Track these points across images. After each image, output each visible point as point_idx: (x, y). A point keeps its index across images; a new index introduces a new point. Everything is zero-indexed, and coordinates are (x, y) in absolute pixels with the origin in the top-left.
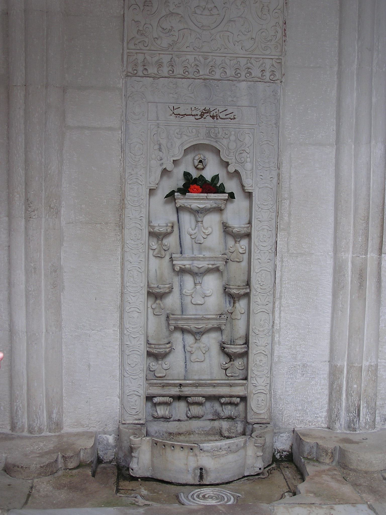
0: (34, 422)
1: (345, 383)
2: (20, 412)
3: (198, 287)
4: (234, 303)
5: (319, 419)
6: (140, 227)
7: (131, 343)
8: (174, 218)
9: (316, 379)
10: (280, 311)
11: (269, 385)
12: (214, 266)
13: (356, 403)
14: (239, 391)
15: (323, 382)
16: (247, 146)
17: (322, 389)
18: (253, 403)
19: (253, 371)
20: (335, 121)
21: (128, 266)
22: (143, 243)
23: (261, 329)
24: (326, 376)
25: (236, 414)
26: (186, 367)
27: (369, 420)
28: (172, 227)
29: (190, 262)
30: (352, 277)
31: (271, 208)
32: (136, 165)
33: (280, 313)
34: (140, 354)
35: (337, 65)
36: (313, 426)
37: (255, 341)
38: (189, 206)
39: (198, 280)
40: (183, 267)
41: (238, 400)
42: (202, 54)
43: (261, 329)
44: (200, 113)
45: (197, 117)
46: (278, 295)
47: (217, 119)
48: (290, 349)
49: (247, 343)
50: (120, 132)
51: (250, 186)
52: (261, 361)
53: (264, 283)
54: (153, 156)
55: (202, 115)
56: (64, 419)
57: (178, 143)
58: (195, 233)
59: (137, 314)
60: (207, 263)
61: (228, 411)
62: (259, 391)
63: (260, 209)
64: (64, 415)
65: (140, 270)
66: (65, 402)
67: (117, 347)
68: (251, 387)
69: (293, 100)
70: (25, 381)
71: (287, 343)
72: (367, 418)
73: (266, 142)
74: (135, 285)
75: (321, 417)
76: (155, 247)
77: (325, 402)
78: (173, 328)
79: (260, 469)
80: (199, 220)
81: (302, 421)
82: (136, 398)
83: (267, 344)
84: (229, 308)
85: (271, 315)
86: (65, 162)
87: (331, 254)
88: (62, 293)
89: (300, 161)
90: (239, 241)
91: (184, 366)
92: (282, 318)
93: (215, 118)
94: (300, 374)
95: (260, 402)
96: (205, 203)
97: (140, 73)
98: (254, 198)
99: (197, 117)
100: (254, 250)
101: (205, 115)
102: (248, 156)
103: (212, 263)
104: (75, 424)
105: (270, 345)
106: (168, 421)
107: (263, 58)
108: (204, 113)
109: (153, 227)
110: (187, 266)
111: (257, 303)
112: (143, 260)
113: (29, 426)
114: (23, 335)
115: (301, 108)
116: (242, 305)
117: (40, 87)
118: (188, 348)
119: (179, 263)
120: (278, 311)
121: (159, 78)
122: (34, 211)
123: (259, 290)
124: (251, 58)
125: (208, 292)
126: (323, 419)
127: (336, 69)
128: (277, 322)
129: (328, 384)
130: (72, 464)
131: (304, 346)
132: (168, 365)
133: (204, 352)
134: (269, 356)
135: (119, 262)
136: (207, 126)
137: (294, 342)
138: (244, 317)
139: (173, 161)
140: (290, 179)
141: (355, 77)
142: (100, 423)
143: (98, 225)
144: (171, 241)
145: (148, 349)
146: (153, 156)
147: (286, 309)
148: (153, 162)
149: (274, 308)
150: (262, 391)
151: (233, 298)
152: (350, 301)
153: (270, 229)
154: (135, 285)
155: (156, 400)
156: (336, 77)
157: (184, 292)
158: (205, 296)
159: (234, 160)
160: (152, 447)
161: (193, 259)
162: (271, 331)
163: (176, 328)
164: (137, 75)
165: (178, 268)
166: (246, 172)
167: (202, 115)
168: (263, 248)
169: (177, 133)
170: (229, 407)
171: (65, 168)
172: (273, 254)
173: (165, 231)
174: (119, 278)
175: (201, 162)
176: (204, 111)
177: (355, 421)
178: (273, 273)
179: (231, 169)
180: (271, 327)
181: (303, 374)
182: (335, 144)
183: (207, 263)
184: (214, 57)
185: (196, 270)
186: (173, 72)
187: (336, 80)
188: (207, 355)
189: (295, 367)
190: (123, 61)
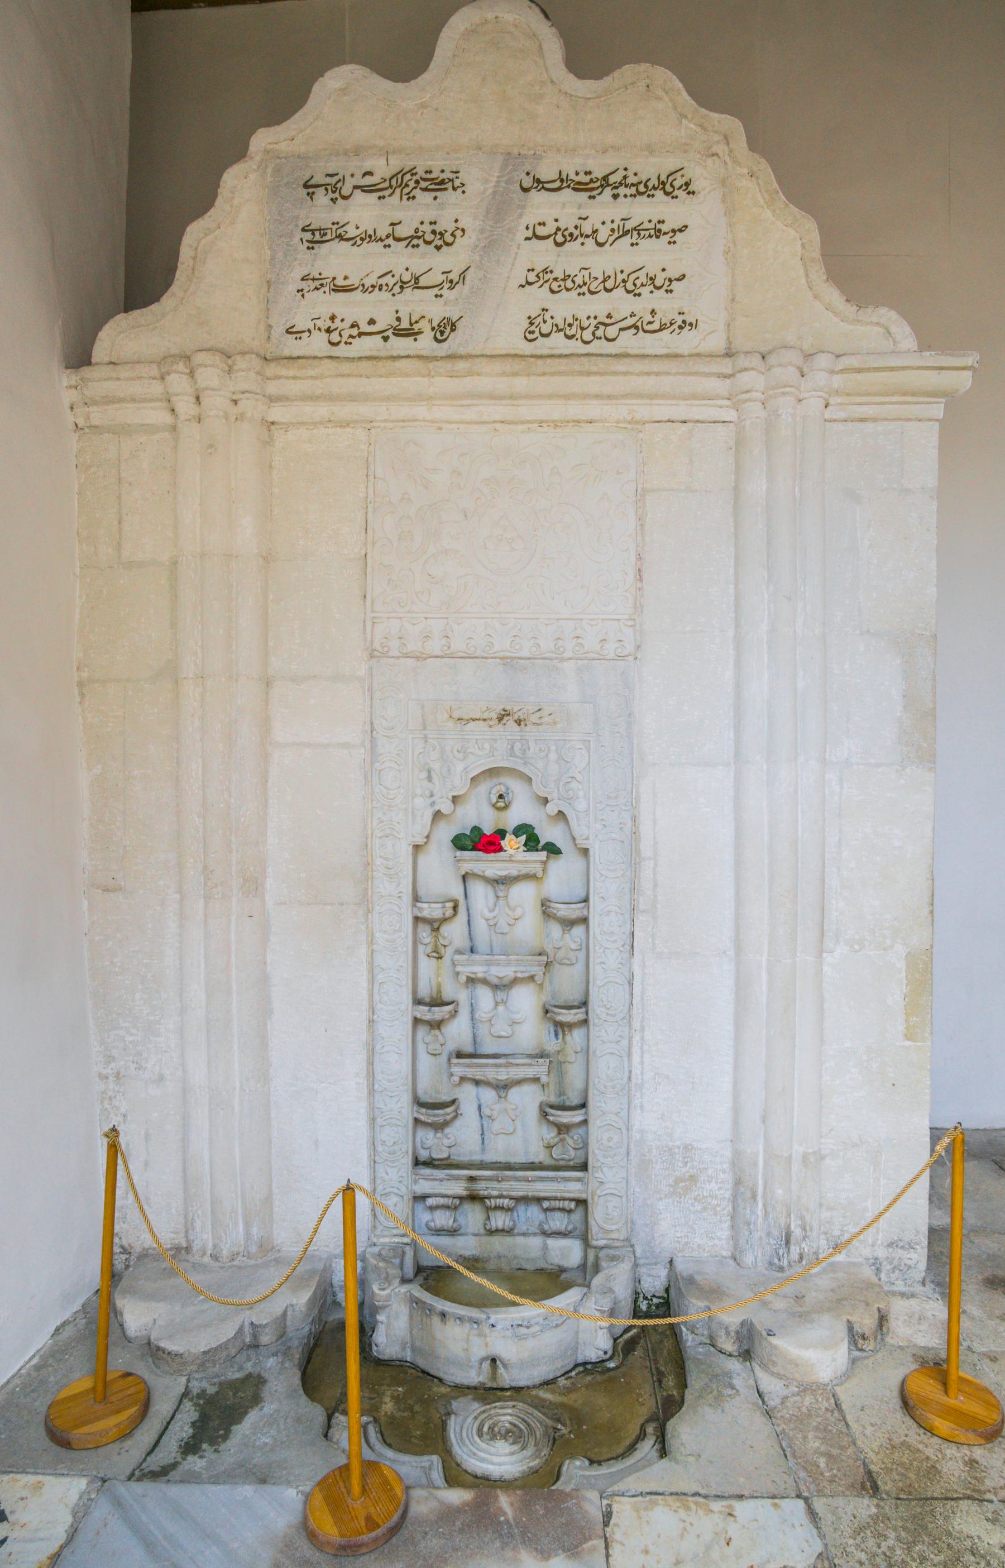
0: (221, 1241)
2: (198, 1224)
3: (501, 1008)
4: (564, 1035)
9: (710, 1172)
10: (642, 1053)
11: (624, 1182)
12: (526, 975)
14: (574, 1189)
15: (722, 1176)
17: (720, 1189)
18: (597, 1214)
19: (596, 1156)
21: (380, 977)
24: (726, 1166)
25: (570, 1228)
26: (483, 1143)
28: (455, 908)
32: (390, 806)
33: (642, 1057)
36: (706, 1255)
37: (599, 1104)
39: (501, 995)
40: (473, 976)
41: (573, 1205)
42: (498, 615)
43: (609, 1084)
44: (495, 716)
45: (491, 723)
50: (362, 751)
54: (419, 791)
55: (500, 719)
57: (460, 767)
58: (494, 917)
60: (514, 969)
61: (558, 1222)
64: (275, 1226)
67: (363, 1111)
68: (593, 1184)
75: (720, 1239)
76: (427, 941)
77: (725, 1212)
78: (456, 1079)
79: (605, 1353)
80: (501, 894)
81: (687, 1243)
82: (395, 1199)
85: (625, 1059)
87: (731, 953)
94: (680, 1164)
98: (591, 859)
99: (491, 723)
100: (595, 946)
101: (506, 718)
102: (580, 787)
103: (522, 969)
105: (626, 1111)
109: (420, 909)
110: (480, 975)
112: (405, 965)
113: (215, 1246)
116: (576, 1037)
117: (223, 679)
118: (486, 1111)
119: (465, 970)
121: (426, 659)
122: (216, 886)
123: (603, 1016)
124: (581, 620)
126: (724, 1242)
127: (731, 633)
128: (637, 1071)
129: (730, 1181)
132: (453, 1139)
134: (625, 1132)
136: (509, 737)
138: (581, 1057)
141: (765, 646)
143: (329, 907)
144: (455, 932)
145: (416, 1115)
146: (419, 791)
148: (419, 801)
151: (561, 1028)
155: (430, 1201)
157: (477, 1016)
158: (514, 1023)
159: (555, 795)
160: (412, 1309)
165: (465, 978)
167: (500, 719)
170: (558, 1215)
172: (626, 955)
175: (501, 797)
177: (781, 1253)
178: (627, 987)
179: (552, 809)
181: (687, 1163)
185: (496, 981)
186: (449, 647)
188: (518, 1122)
189: (670, 1150)
190: (365, 631)
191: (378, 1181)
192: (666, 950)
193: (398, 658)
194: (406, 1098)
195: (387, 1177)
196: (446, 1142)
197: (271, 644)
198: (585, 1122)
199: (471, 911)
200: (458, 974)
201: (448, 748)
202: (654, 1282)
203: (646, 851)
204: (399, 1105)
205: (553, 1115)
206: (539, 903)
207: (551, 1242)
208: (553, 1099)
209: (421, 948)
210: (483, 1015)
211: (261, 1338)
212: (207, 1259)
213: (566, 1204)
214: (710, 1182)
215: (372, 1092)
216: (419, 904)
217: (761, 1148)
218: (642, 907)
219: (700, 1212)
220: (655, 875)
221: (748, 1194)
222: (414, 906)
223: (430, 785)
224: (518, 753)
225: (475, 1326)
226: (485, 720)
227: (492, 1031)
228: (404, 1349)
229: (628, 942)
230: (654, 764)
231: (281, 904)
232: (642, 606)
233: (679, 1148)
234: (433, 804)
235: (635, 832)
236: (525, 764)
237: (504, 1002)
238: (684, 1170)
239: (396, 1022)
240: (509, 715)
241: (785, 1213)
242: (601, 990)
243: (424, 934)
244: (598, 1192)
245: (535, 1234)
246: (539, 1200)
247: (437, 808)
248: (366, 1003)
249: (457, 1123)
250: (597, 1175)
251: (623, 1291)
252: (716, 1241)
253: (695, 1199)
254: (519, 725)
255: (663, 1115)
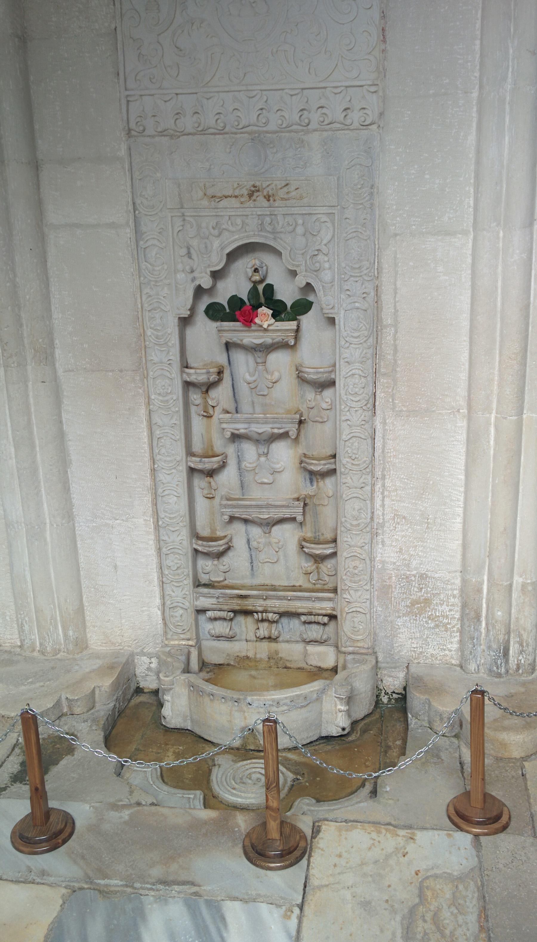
1: (484, 605)
5: (447, 652)
6: (169, 375)
7: (169, 538)
8: (222, 359)
9: (442, 596)
10: (384, 497)
11: (368, 602)
12: (281, 431)
13: (501, 637)
14: (327, 607)
16: (325, 242)
18: (347, 625)
19: (345, 581)
20: (472, 190)
21: (158, 433)
22: (174, 398)
23: (355, 523)
25: (325, 637)
26: (252, 569)
27: (522, 662)
28: (220, 373)
29: (246, 426)
30: (494, 449)
31: (365, 342)
33: (383, 500)
34: (182, 553)
35: (477, 87)
36: (438, 662)
37: (345, 539)
38: (239, 342)
39: (263, 449)
44: (245, 192)
45: (242, 200)
46: (380, 473)
47: (274, 201)
48: (400, 552)
49: (335, 541)
50: (128, 230)
51: (331, 307)
52: (355, 568)
53: (357, 456)
54: (180, 267)
55: (250, 195)
56: (89, 635)
57: (216, 244)
58: (255, 381)
59: (175, 498)
60: (271, 426)
61: (315, 632)
62: (354, 609)
63: (348, 344)
64: (88, 630)
65: (173, 438)
66: (87, 613)
67: (151, 542)
69: (398, 158)
70: (30, 587)
71: (394, 544)
72: (520, 658)
73: (354, 234)
74: (168, 459)
75: (450, 651)
76: (197, 402)
78: (226, 517)
80: (259, 360)
81: (421, 653)
82: (181, 612)
83: (364, 545)
84: (309, 490)
85: (368, 502)
86: (52, 280)
87: (464, 411)
88: (69, 470)
89: (411, 264)
90: (321, 392)
91: (250, 568)
92: (386, 507)
93: (271, 199)
94: (416, 589)
95: (356, 625)
96: (262, 337)
97: (150, 131)
99: (242, 200)
101: (256, 194)
102: (326, 259)
104: (104, 641)
106: (231, 641)
107: (347, 87)
108: (253, 192)
109: (189, 374)
110: (242, 431)
111: (347, 485)
114: (20, 527)
115: (413, 171)
116: (328, 483)
118: (254, 544)
119: (230, 428)
120: (380, 496)
121: (179, 137)
123: (349, 466)
124: (325, 88)
125: (278, 466)
128: (378, 512)
129: (460, 604)
130: (79, 709)
131: (420, 549)
133: (277, 550)
134: (368, 562)
135: (144, 425)
136: (259, 213)
137: (405, 542)
139: (211, 272)
140: (396, 293)
142: (137, 641)
145: (195, 546)
146: (180, 267)
147: (393, 494)
148: (181, 276)
149: (373, 491)
150: (358, 609)
151: (314, 476)
152: (492, 487)
153: (364, 375)
154: (168, 459)
155: (209, 614)
156: (475, 109)
157: (243, 466)
158: (274, 472)
159: (303, 268)
161: (249, 421)
162: (369, 526)
163: (232, 519)
164: (145, 133)
166: (323, 286)
167: (250, 195)
168: (354, 403)
169: (213, 228)
170: (314, 627)
171: (53, 290)
173: (205, 380)
174: (146, 448)
175: (256, 270)
176: (253, 189)
177: (499, 663)
178: (369, 441)
179: (301, 281)
180: (369, 520)
181: (422, 588)
182: (471, 230)
183: (271, 426)
184: (264, 93)
185: (256, 436)
187: (474, 115)
188: (281, 553)
189: (407, 577)
191: (167, 598)
192: (404, 409)
193: (153, 137)
194: (185, 533)
195: (173, 594)
196: (222, 568)
197: (37, 127)
198: (334, 554)
199: (234, 377)
200: (224, 429)
201: (204, 225)
202: (393, 682)
203: (387, 320)
204: (180, 538)
205: (307, 548)
206: (294, 368)
207: (310, 648)
208: (309, 535)
209: (193, 409)
210: (248, 465)
211: (75, 708)
212: (36, 654)
213: (320, 619)
214: (442, 605)
215: (157, 527)
216: (187, 370)
217: (486, 578)
218: (382, 370)
219: (433, 628)
220: (395, 340)
221: (472, 614)
222: (182, 372)
223: (190, 261)
224: (269, 228)
225: (236, 704)
226: (236, 197)
227: (257, 478)
228: (185, 721)
229: (371, 401)
230: (396, 235)
231: (70, 371)
232: (385, 70)
233: (415, 576)
234: (193, 279)
235: (378, 301)
236: (275, 239)
237: (266, 454)
238: (419, 594)
239: (173, 471)
240: (258, 191)
241: (503, 631)
242: (347, 443)
243: (195, 396)
244: (346, 609)
245: (297, 642)
246: (297, 615)
247: (197, 283)
248: (147, 455)
249: (230, 554)
250: (345, 596)
251: (363, 686)
252: (447, 652)
253: (429, 618)
254: (269, 200)
255: (401, 549)
